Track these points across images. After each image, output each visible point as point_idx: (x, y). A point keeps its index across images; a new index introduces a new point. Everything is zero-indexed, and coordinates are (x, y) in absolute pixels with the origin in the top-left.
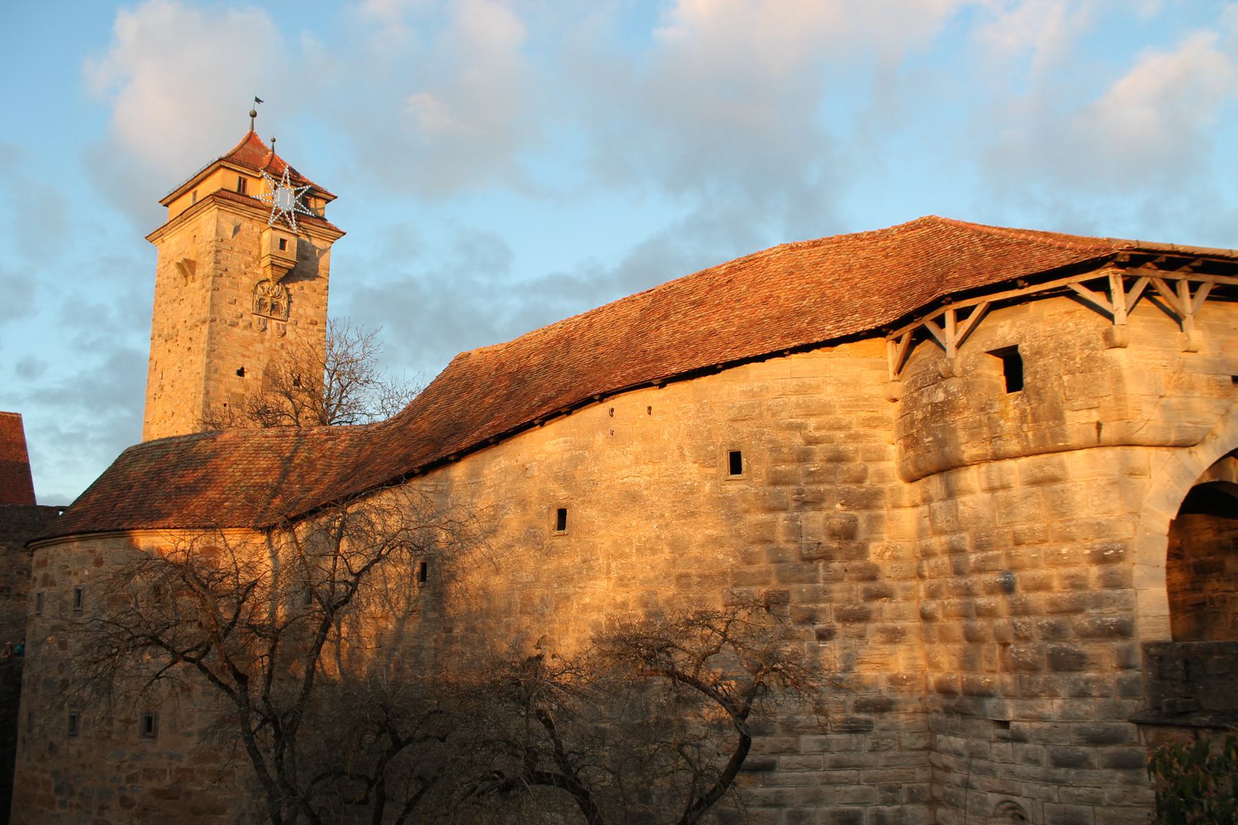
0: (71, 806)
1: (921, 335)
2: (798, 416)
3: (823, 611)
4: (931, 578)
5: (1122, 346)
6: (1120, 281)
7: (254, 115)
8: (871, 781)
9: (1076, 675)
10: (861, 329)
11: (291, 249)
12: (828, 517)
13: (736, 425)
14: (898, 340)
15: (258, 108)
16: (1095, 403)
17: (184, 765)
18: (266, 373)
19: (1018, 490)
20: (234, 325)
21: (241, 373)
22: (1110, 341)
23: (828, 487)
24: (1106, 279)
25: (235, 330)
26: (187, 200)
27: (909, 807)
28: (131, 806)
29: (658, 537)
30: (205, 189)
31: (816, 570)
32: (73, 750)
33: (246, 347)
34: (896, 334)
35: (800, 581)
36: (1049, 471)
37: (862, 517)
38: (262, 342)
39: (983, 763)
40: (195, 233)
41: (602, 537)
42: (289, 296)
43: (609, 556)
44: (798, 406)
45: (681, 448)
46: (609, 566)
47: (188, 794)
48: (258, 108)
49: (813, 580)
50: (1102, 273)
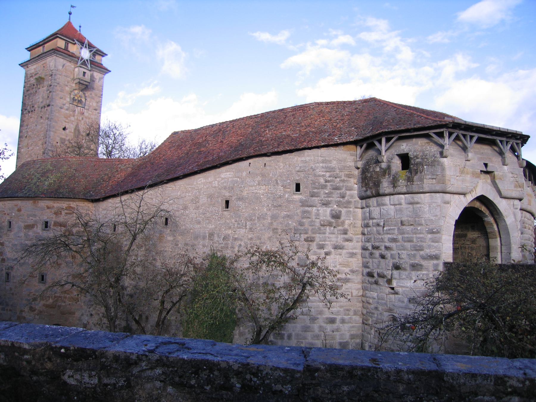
0: (7, 310)
1: (371, 146)
2: (322, 172)
3: (327, 245)
4: (368, 234)
5: (446, 157)
6: (448, 134)
7: (70, 14)
8: (341, 307)
9: (419, 273)
10: (348, 140)
11: (88, 76)
12: (331, 210)
13: (299, 173)
14: (361, 147)
15: (72, 10)
16: (435, 177)
17: (58, 295)
18: (75, 129)
19: (404, 206)
20: (61, 108)
21: (64, 129)
22: (442, 155)
23: (332, 199)
24: (443, 132)
25: (63, 110)
26: (40, 50)
27: (354, 317)
28: (35, 310)
29: (266, 214)
30: (48, 46)
31: (325, 230)
32: (8, 288)
33: (67, 118)
34: (361, 144)
35: (320, 233)
36: (416, 200)
37: (344, 211)
38: (74, 116)
39: (384, 301)
40: (44, 65)
41: (244, 212)
42: (85, 97)
43: (246, 219)
44: (323, 167)
45: (277, 181)
46: (246, 223)
47: (60, 306)
48: (72, 10)
49: (324, 233)
50: (442, 130)
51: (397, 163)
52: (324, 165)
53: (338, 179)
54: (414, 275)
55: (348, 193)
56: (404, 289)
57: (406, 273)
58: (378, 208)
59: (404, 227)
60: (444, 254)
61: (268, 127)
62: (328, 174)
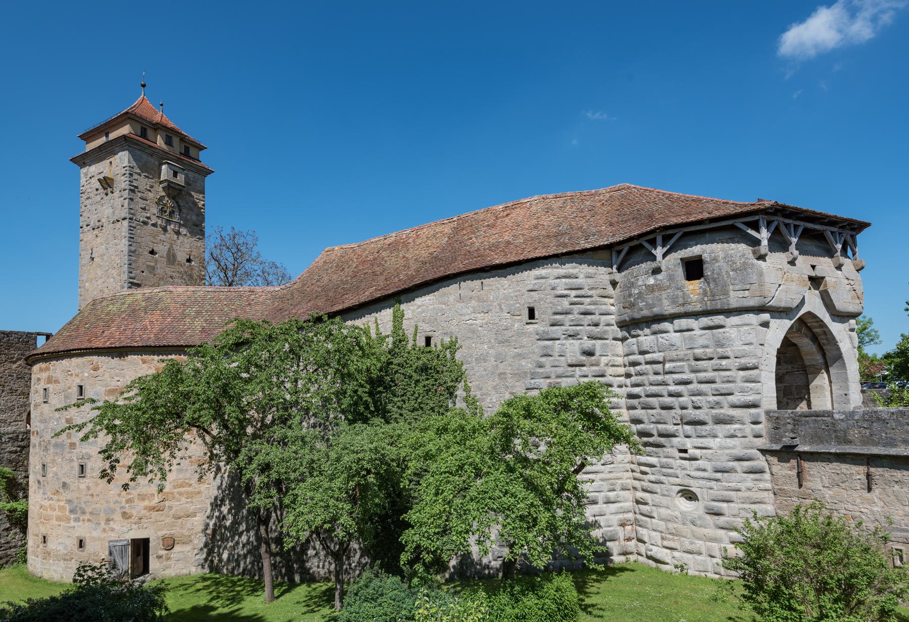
12: (581, 344)
13: (532, 293)
14: (619, 252)
44: (566, 284)
51: (680, 272)
52: (567, 280)
53: (588, 300)
54: (721, 429)
55: (603, 318)
56: (704, 451)
57: (707, 427)
58: (653, 337)
59: (698, 363)
60: (765, 399)
61: (474, 233)
62: (573, 293)
